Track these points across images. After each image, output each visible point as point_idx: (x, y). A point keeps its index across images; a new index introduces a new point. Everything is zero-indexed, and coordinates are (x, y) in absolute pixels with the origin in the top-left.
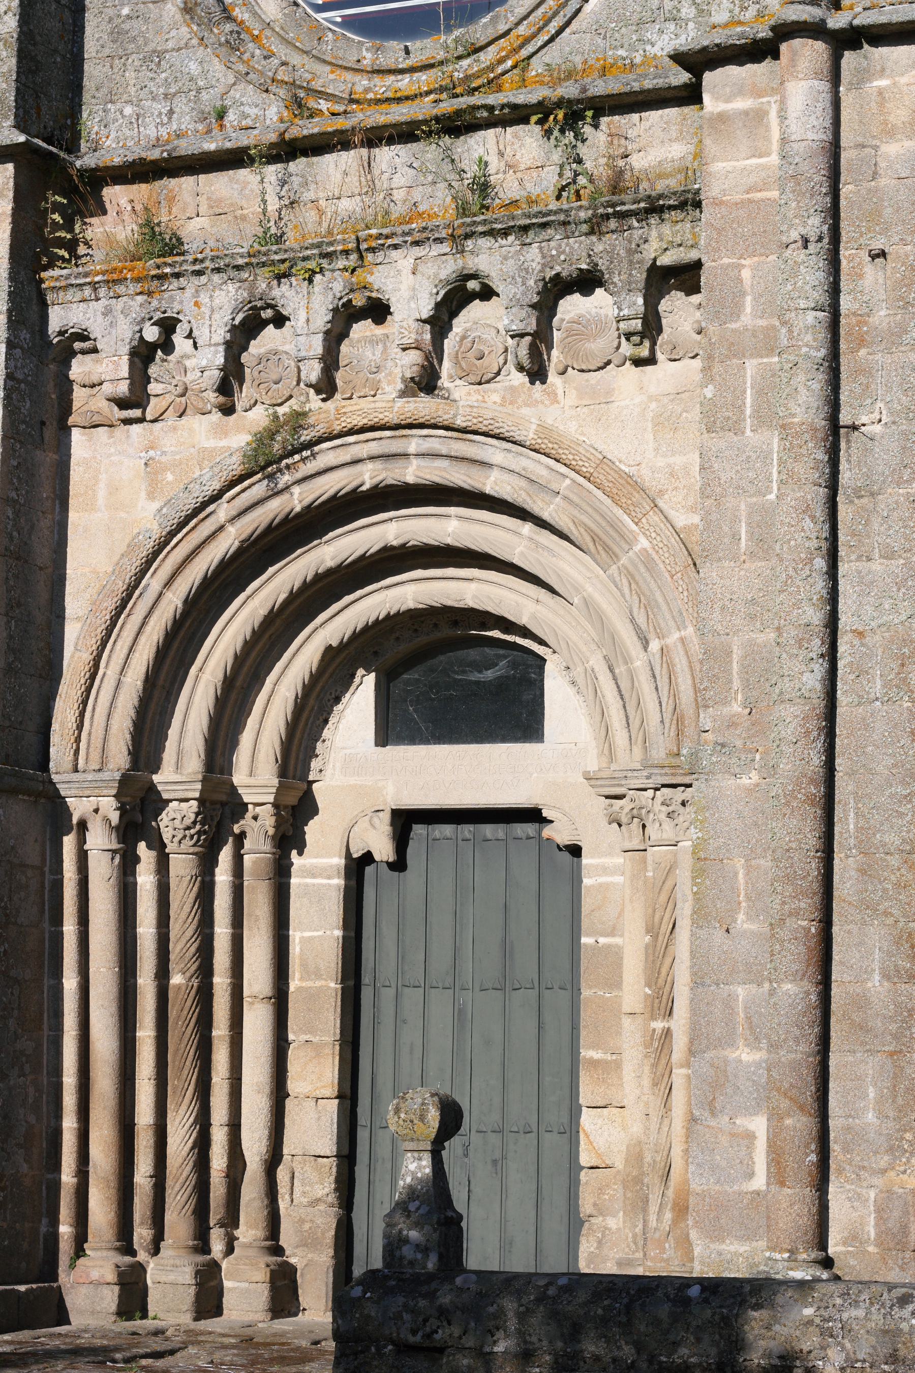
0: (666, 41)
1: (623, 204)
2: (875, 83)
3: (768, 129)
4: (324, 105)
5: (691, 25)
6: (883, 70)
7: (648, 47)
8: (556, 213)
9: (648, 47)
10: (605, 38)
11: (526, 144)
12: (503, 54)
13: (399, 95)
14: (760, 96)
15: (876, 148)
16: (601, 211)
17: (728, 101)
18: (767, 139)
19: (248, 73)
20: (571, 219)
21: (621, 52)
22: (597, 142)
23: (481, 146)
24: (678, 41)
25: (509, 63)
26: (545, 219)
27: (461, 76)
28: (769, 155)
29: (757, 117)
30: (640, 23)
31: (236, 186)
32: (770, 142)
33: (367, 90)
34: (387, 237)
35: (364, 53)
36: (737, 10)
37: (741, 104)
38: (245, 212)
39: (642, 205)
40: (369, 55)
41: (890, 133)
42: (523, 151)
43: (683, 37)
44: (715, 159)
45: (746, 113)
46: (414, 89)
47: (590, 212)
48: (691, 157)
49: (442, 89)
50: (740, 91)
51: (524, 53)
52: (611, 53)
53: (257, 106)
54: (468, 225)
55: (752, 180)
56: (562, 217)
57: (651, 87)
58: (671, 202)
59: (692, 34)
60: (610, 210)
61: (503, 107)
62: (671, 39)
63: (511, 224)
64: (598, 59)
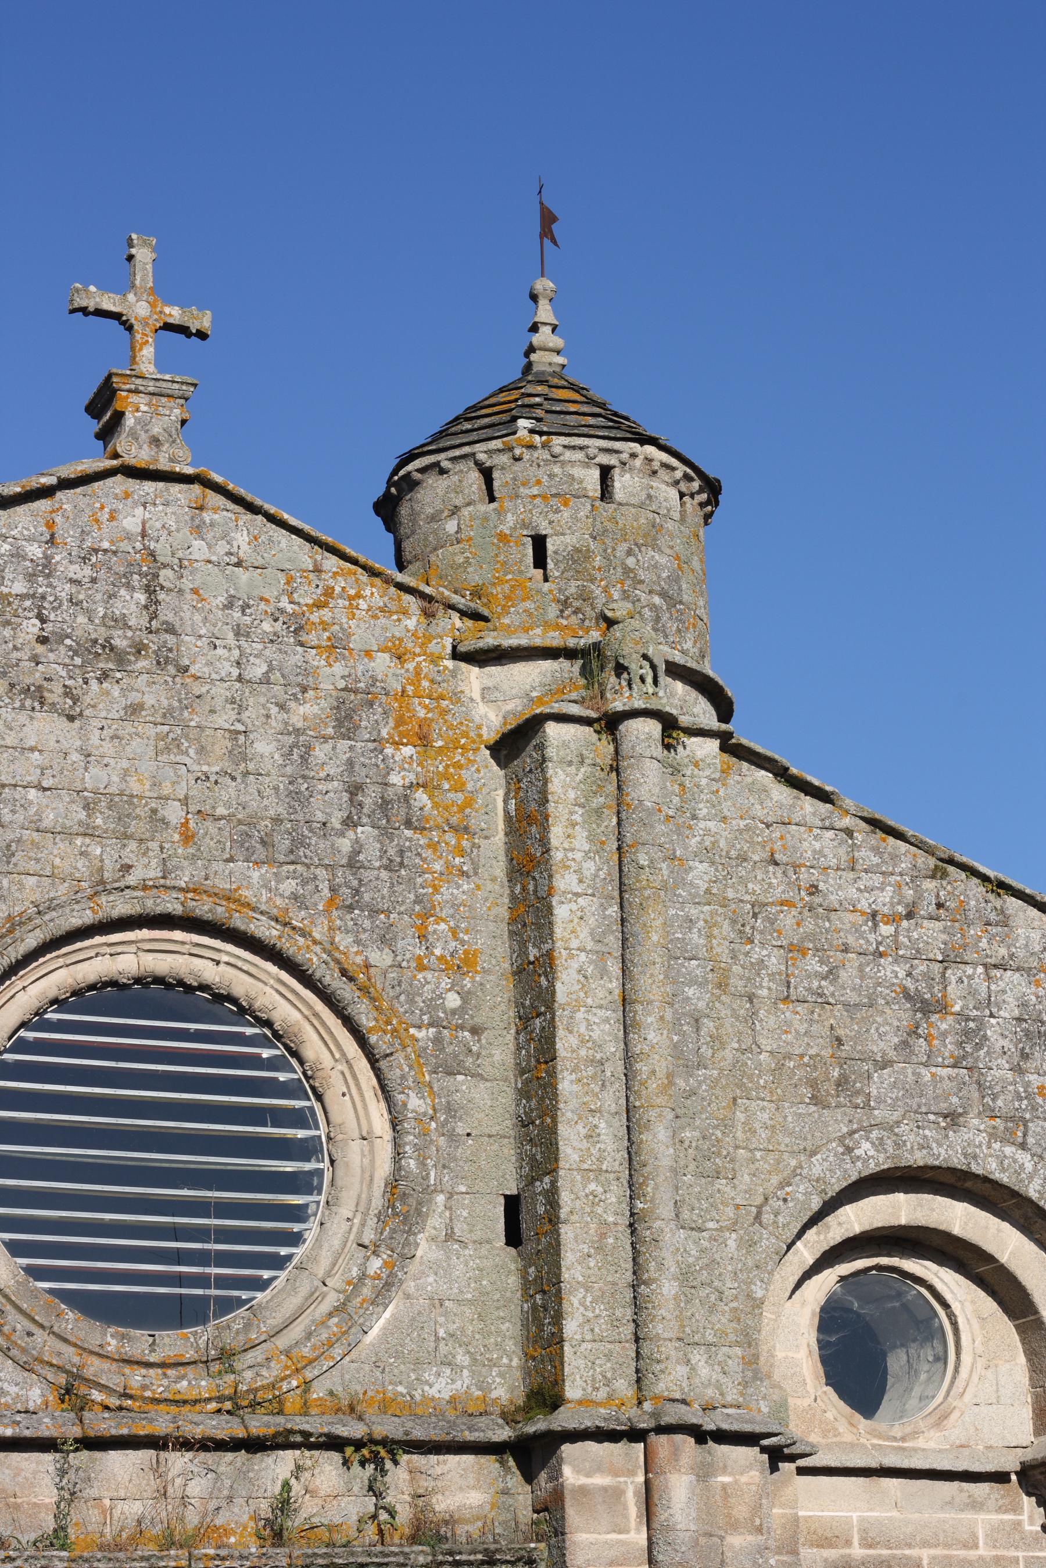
0: (443, 1385)
1: (460, 1553)
2: (720, 1479)
3: (626, 1508)
4: (97, 1396)
5: (466, 1372)
6: (725, 1466)
7: (426, 1388)
8: (396, 1554)
9: (426, 1388)
10: (383, 1372)
11: (327, 1471)
12: (288, 1372)
13: (178, 1397)
14: (617, 1476)
15: (722, 1538)
16: (440, 1558)
17: (588, 1476)
18: (626, 1517)
19: (9, 1349)
20: (410, 1563)
21: (400, 1389)
22: (400, 1478)
23: (279, 1465)
24: (454, 1386)
25: (295, 1383)
26: (386, 1560)
27: (245, 1388)
28: (628, 1532)
29: (615, 1494)
30: (417, 1362)
31: (7, 1471)
32: (628, 1520)
33: (144, 1387)
34: (223, 1559)
35: (109, 1339)
36: (590, 1390)
37: (599, 1480)
38: (19, 1500)
39: (480, 1557)
40: (114, 1342)
41: (734, 1526)
42: (322, 1478)
43: (459, 1383)
44: (578, 1529)
45: (605, 1489)
46: (194, 1394)
47: (430, 1558)
48: (488, 1507)
49: (220, 1399)
50: (598, 1468)
51: (309, 1374)
52: (390, 1388)
53: (17, 1385)
54: (308, 1556)
55: (612, 1553)
56: (401, 1560)
57: (472, 1439)
58: (508, 1558)
59: (467, 1382)
60: (451, 1559)
61: (321, 1435)
62: (447, 1384)
63: (352, 1560)
64: (378, 1392)
